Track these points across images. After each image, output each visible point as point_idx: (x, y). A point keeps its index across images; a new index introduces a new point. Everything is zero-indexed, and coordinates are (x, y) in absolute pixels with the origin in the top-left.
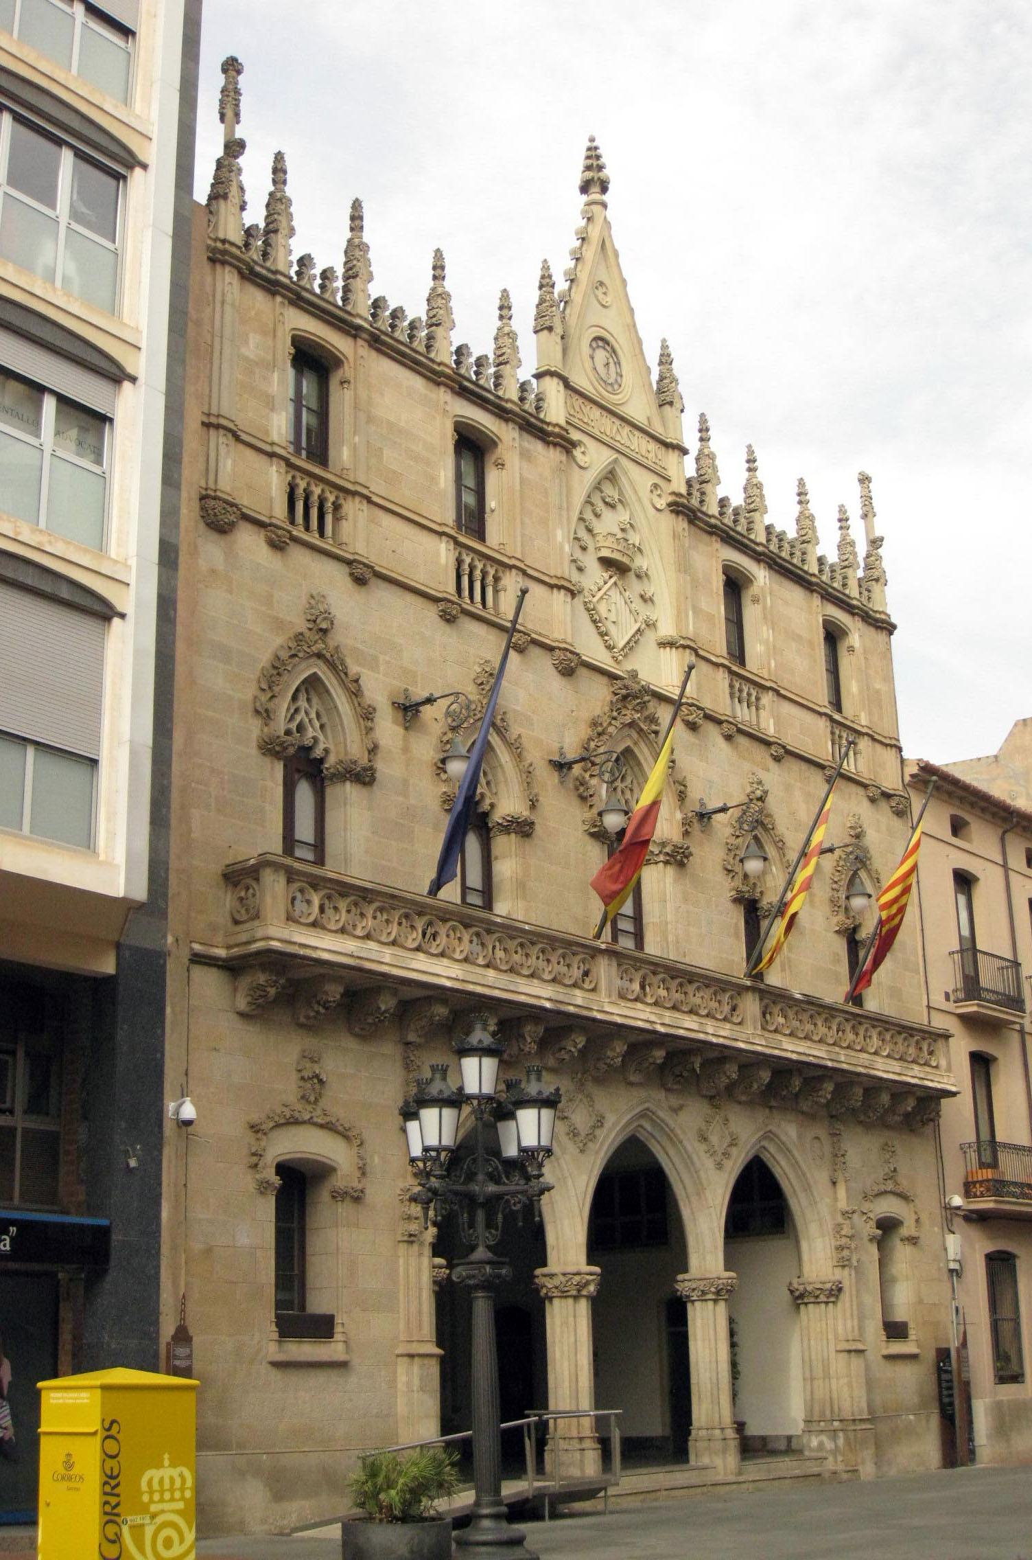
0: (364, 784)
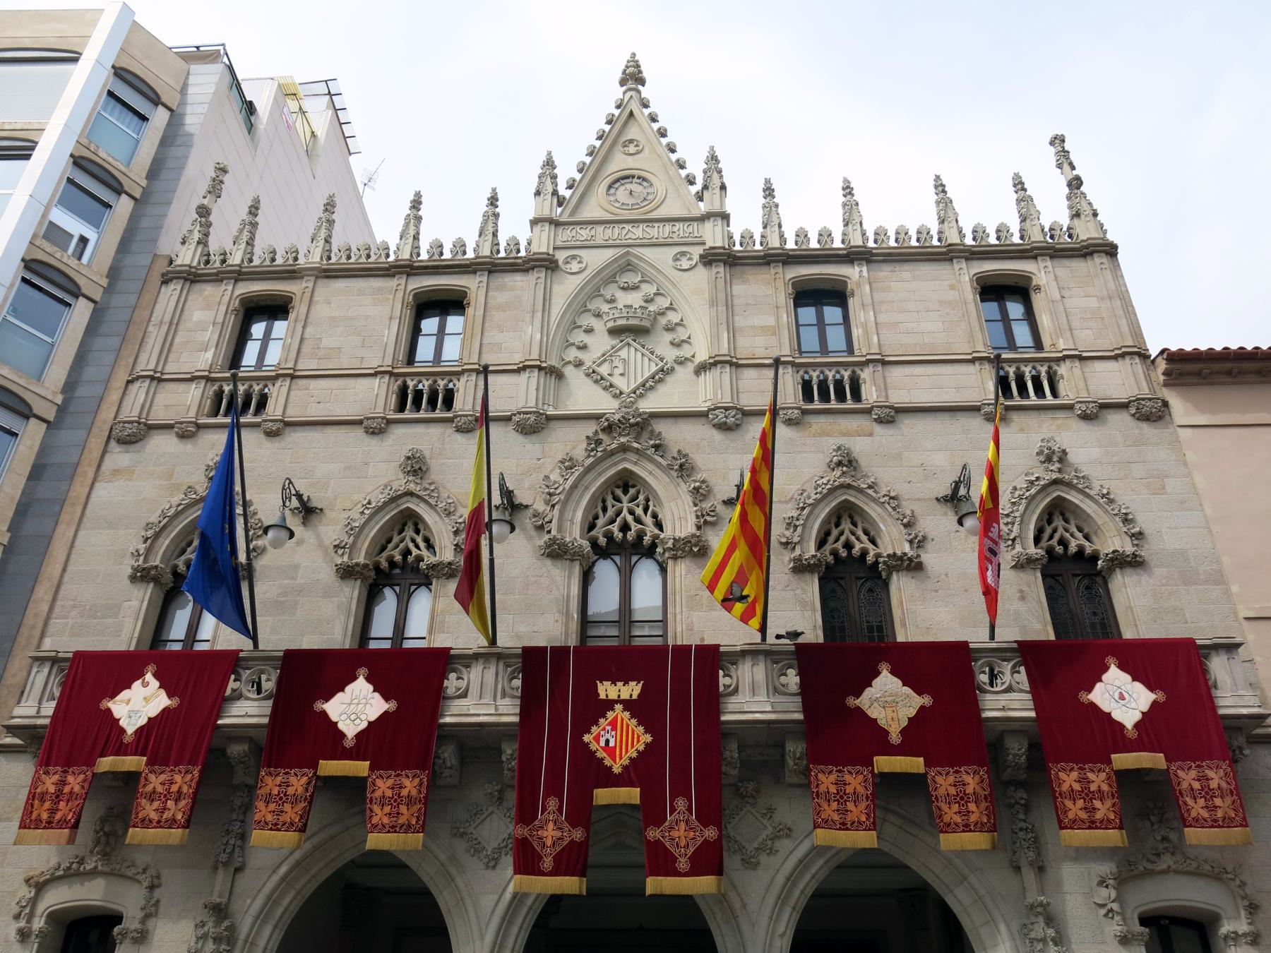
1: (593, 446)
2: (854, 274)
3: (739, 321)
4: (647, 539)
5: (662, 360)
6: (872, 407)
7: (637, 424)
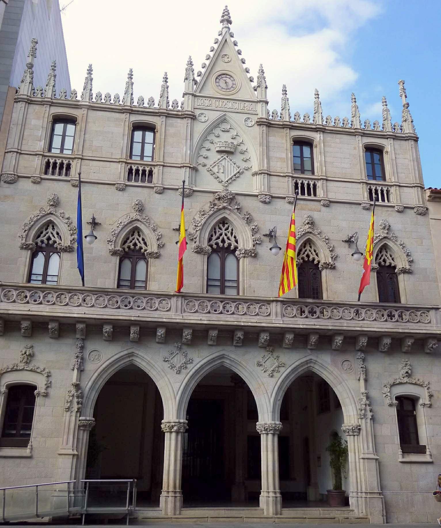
0: (70, 252)
1: (212, 206)
2: (317, 137)
3: (271, 154)
4: (232, 247)
5: (239, 168)
6: (322, 200)
7: (230, 198)
